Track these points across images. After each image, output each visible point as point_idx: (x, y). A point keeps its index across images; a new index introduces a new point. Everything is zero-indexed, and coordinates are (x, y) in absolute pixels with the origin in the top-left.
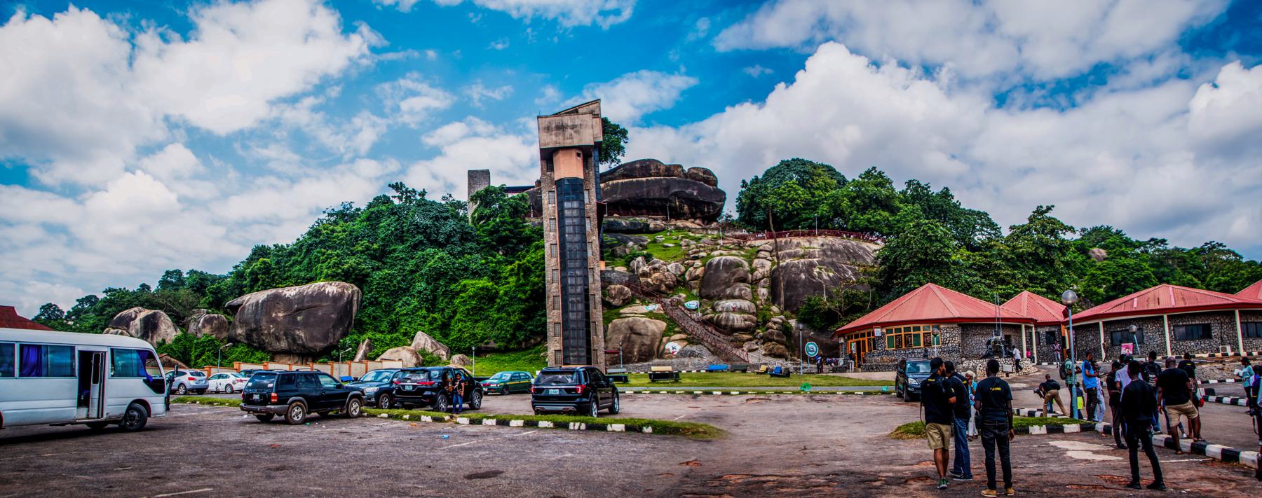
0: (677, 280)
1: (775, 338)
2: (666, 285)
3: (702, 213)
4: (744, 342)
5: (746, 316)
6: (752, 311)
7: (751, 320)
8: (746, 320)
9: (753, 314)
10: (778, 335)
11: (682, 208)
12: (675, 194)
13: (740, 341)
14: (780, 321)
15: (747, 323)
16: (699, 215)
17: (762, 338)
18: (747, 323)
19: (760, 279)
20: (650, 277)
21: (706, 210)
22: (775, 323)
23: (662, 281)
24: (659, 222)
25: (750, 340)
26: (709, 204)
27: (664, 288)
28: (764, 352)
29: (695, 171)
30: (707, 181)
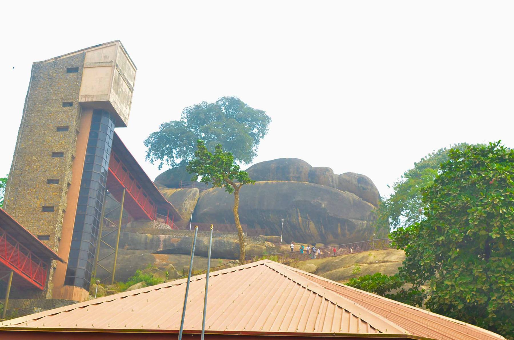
3: (336, 235)
16: (330, 237)
21: (339, 230)
24: (258, 243)
26: (343, 222)
29: (347, 178)
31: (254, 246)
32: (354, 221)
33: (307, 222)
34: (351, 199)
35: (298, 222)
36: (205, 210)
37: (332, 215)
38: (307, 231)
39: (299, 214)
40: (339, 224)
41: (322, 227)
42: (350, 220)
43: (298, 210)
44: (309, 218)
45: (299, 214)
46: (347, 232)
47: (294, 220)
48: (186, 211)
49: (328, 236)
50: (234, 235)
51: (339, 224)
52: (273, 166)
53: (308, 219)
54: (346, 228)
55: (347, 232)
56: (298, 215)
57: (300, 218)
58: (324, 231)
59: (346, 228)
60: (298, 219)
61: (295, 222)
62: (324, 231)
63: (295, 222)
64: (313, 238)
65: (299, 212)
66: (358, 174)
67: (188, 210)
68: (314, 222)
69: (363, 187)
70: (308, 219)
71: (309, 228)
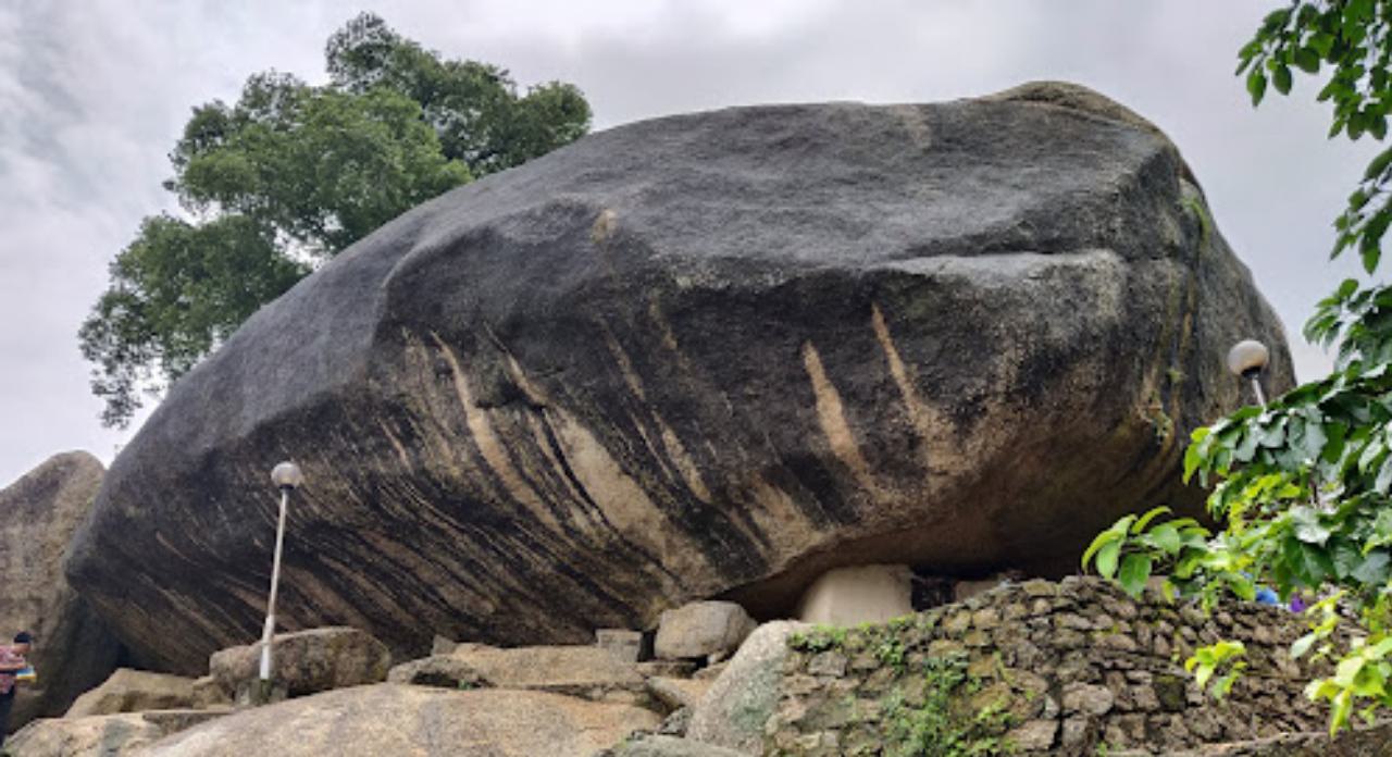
33: (543, 442)
35: (479, 459)
37: (705, 277)
38: (579, 519)
39: (461, 382)
40: (812, 358)
41: (669, 437)
43: (447, 353)
44: (537, 395)
45: (461, 382)
46: (926, 418)
47: (445, 445)
49: (759, 518)
51: (812, 358)
54: (897, 369)
55: (926, 418)
56: (453, 398)
57: (477, 422)
58: (693, 477)
59: (897, 369)
60: (463, 431)
61: (456, 472)
62: (693, 477)
64: (650, 568)
65: (454, 363)
68: (584, 419)
70: (537, 409)
71: (578, 485)
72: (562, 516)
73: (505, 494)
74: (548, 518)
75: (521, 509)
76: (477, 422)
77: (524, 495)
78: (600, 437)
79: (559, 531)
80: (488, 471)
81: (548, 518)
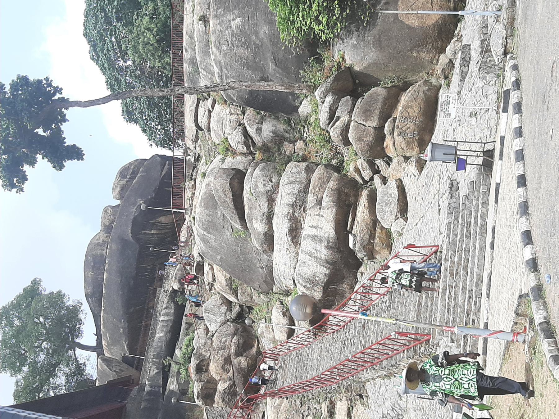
0: (233, 321)
1: (374, 123)
2: (238, 354)
4: (375, 222)
5: (311, 198)
6: (304, 174)
7: (321, 187)
8: (319, 202)
9: (309, 171)
10: (367, 113)
11: (163, 226)
12: (135, 234)
13: (372, 236)
14: (329, 99)
15: (326, 201)
17: (372, 165)
18: (326, 201)
19: (245, 133)
20: (215, 383)
22: (332, 117)
23: (227, 361)
25: (372, 198)
27: (243, 361)
28: (412, 168)
29: (118, 189)
30: (134, 174)
31: (175, 278)
32: (164, 172)
34: (140, 174)
36: (126, 347)
38: (168, 227)
39: (147, 232)
40: (166, 188)
42: (163, 175)
45: (147, 232)
48: (122, 371)
50: (159, 303)
51: (166, 188)
52: (90, 273)
53: (155, 222)
57: (153, 232)
61: (156, 238)
63: (156, 238)
66: (116, 178)
67: (122, 369)
68: (160, 217)
69: (132, 174)
72: (167, 229)
73: (162, 234)
74: (167, 231)
75: (164, 233)
76: (153, 232)
77: (163, 231)
78: (163, 216)
79: (168, 231)
80: (158, 234)
81: (167, 231)
